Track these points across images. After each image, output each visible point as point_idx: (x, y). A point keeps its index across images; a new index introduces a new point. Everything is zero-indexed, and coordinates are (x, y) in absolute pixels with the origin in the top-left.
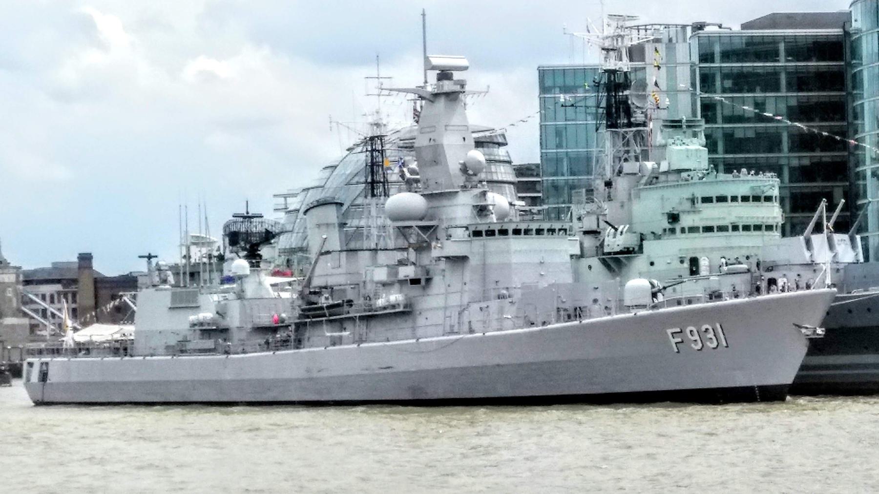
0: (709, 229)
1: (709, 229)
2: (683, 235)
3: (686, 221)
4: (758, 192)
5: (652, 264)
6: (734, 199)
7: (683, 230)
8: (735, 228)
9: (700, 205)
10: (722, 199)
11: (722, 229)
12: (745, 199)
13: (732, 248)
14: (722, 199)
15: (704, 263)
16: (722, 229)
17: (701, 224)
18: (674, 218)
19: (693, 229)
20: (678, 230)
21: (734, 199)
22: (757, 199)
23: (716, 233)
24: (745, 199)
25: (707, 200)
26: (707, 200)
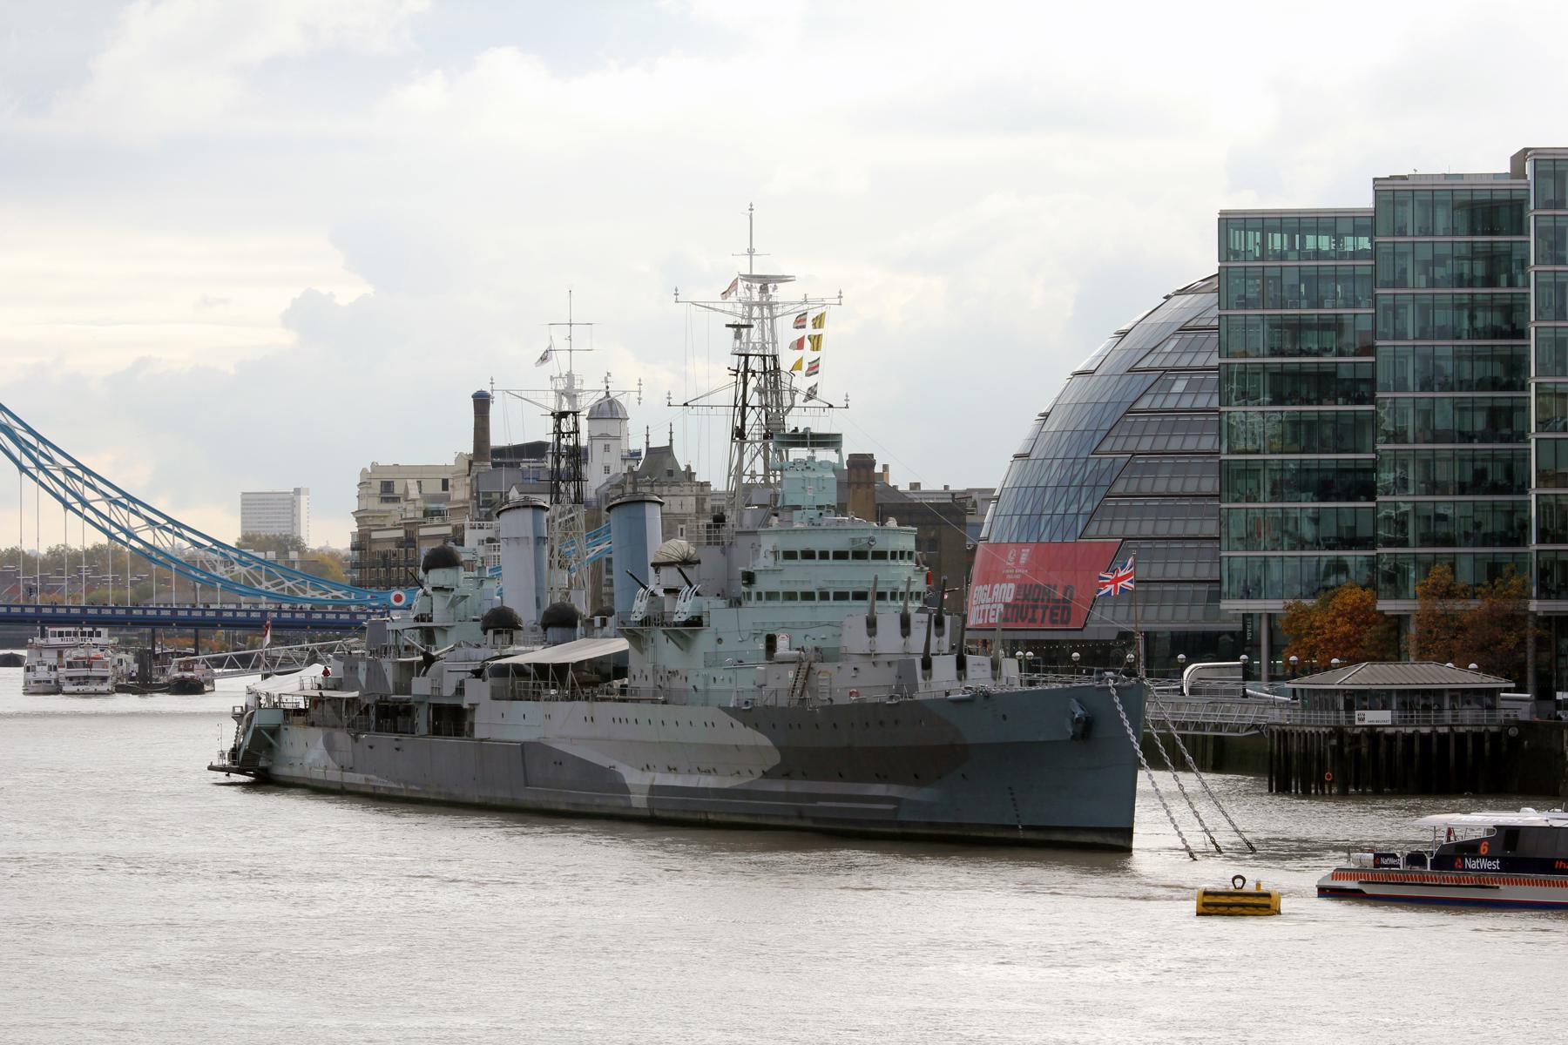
0: (791, 596)
1: (791, 596)
2: (760, 604)
3: (763, 584)
4: (862, 546)
5: (720, 641)
6: (824, 555)
7: (759, 596)
8: (824, 596)
9: (782, 562)
10: (808, 555)
11: (808, 596)
12: (840, 555)
13: (819, 624)
14: (808, 555)
15: (782, 646)
16: (808, 596)
17: (781, 589)
18: (749, 578)
19: (771, 596)
20: (754, 596)
21: (824, 555)
22: (860, 555)
23: (799, 603)
24: (840, 555)
25: (790, 555)
26: (790, 555)
